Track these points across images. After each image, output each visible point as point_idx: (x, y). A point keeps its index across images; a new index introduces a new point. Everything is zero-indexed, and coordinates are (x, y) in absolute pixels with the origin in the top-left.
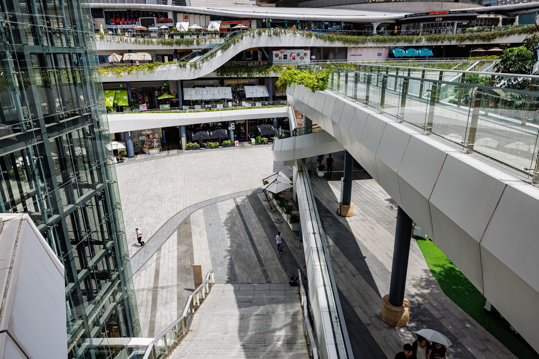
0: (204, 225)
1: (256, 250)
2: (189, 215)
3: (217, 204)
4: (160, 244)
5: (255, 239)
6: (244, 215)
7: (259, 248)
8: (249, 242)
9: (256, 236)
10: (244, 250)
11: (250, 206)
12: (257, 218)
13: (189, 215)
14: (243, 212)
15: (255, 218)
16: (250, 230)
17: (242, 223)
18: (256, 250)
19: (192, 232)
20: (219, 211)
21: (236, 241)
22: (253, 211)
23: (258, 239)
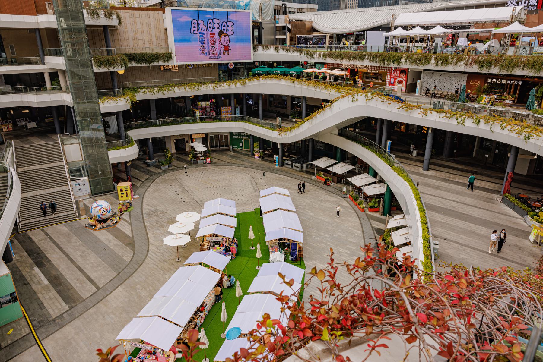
0: (112, 248)
1: (55, 242)
2: (134, 251)
3: (115, 274)
4: (133, 226)
5: (57, 250)
6: (76, 269)
7: (52, 244)
8: (62, 246)
9: (57, 253)
10: (64, 240)
11: (73, 285)
12: (60, 270)
13: (134, 251)
14: (79, 273)
15: (62, 269)
16: (64, 256)
17: (75, 260)
18: (55, 242)
19: (116, 239)
20: (106, 265)
21: (73, 244)
22: (67, 277)
23: (54, 251)
